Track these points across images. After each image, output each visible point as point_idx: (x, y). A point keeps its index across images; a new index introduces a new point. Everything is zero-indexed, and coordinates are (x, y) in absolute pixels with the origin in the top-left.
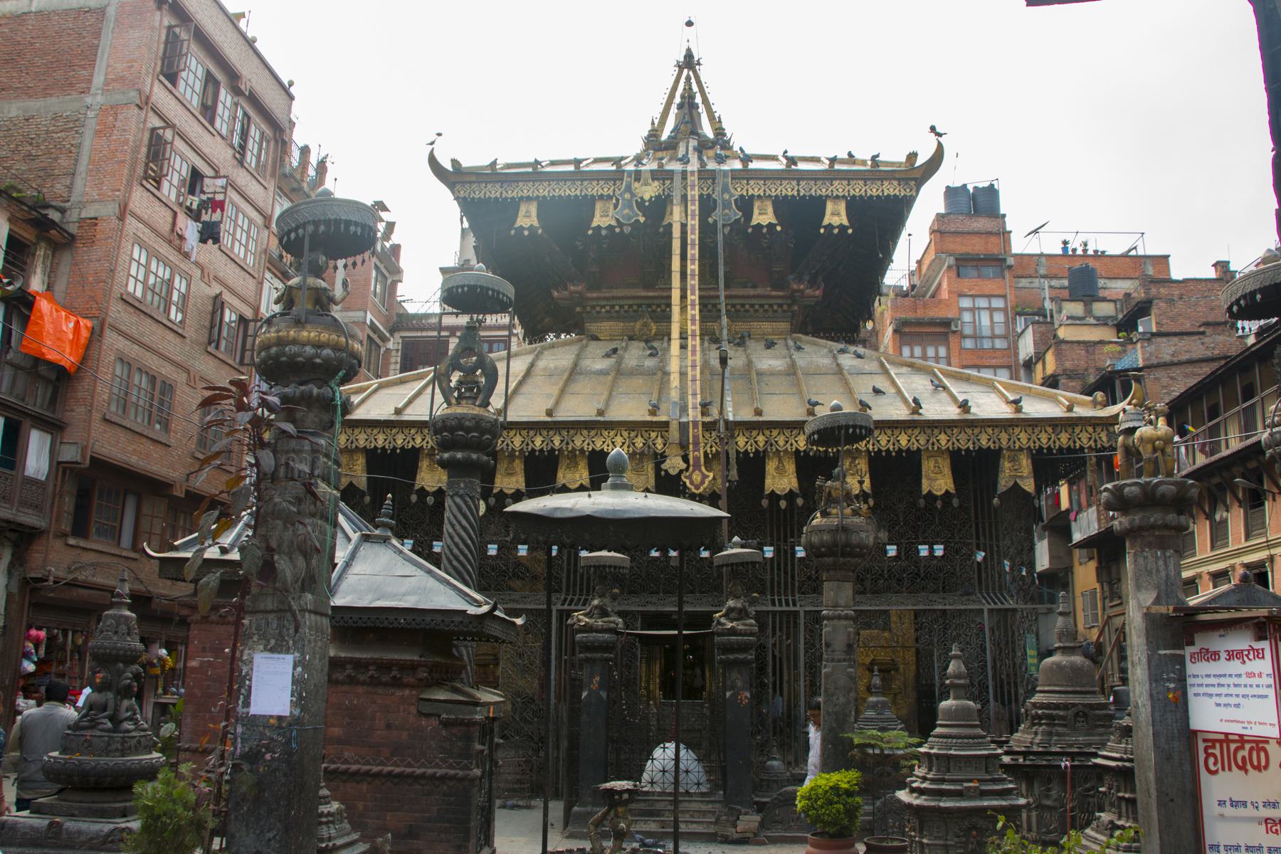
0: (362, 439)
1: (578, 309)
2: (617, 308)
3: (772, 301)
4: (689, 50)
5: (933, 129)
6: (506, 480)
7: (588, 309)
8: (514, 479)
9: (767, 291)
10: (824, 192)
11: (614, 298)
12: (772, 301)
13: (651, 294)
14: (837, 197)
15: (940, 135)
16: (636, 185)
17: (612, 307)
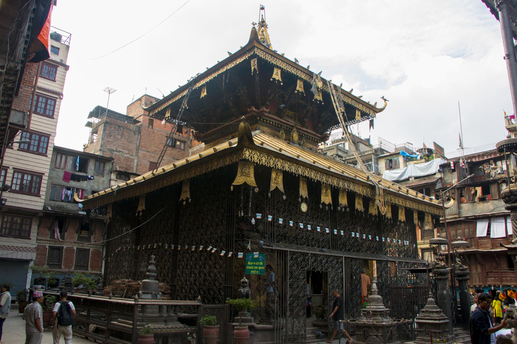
0: (287, 167)
1: (258, 118)
2: (271, 123)
3: (315, 137)
4: (262, 19)
5: (383, 97)
6: (325, 198)
7: (262, 119)
8: (327, 198)
9: (314, 133)
10: (357, 106)
11: (269, 117)
12: (315, 137)
13: (282, 120)
14: (360, 110)
15: (385, 100)
16: (316, 80)
17: (270, 121)
